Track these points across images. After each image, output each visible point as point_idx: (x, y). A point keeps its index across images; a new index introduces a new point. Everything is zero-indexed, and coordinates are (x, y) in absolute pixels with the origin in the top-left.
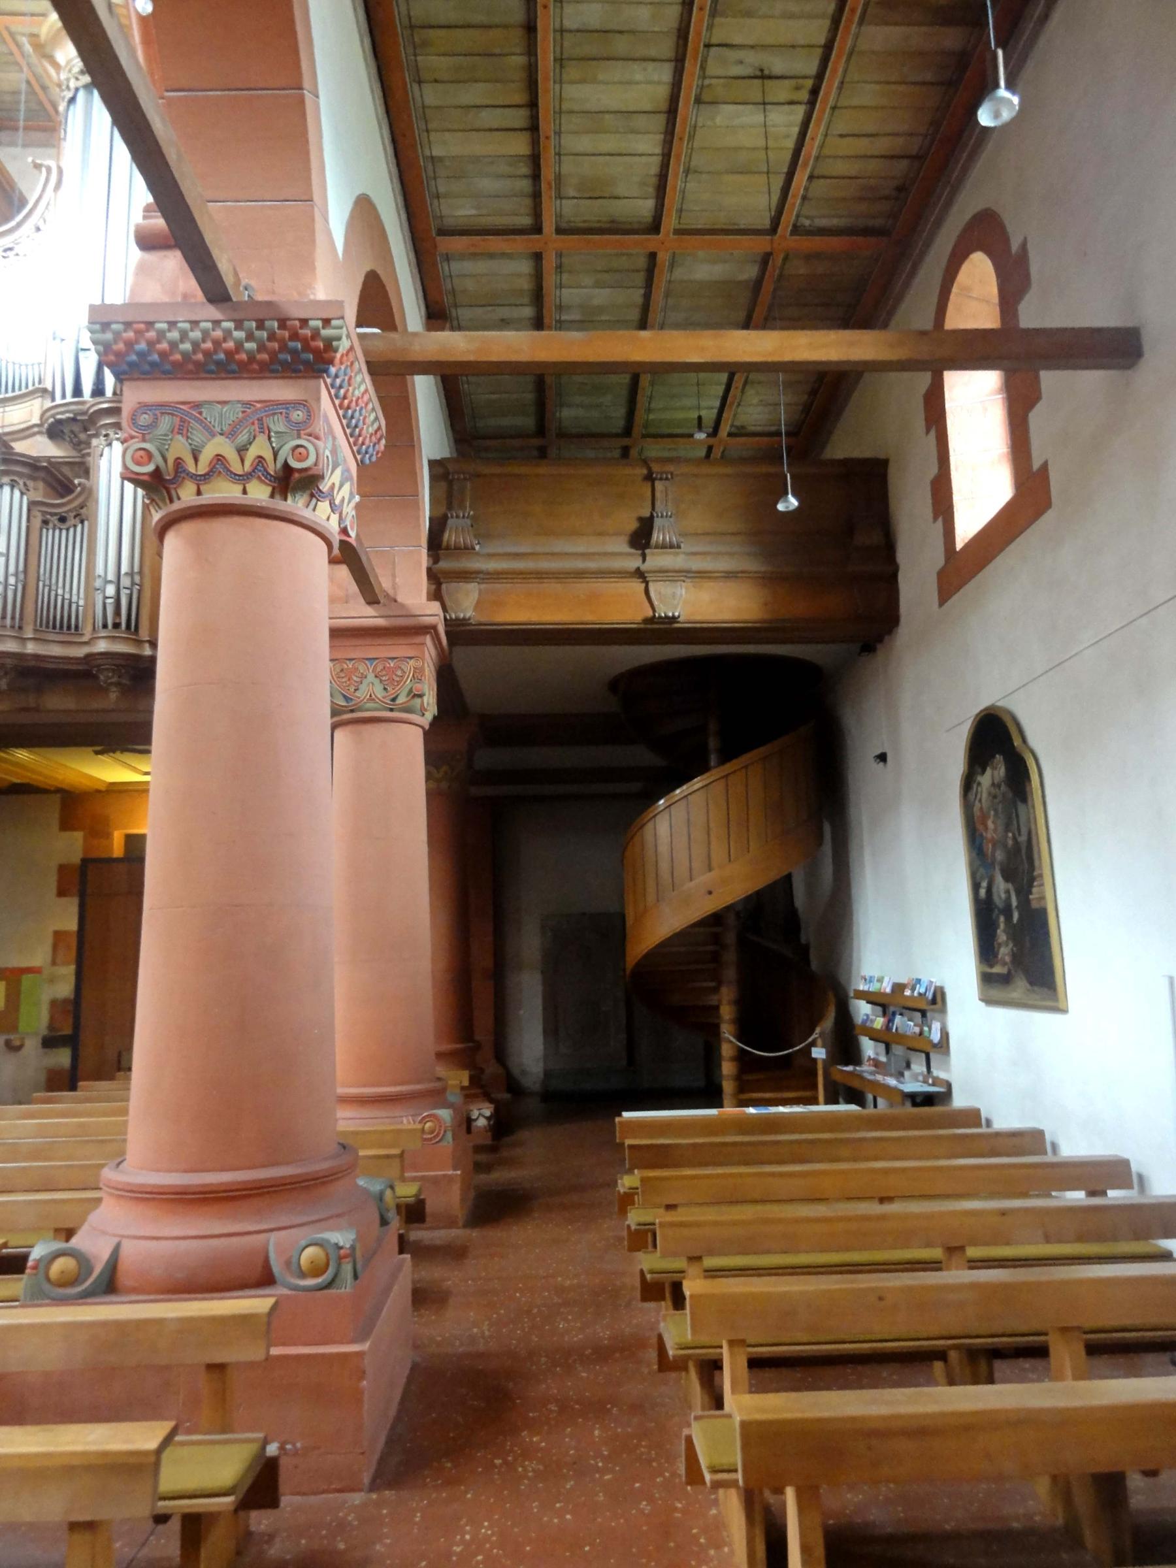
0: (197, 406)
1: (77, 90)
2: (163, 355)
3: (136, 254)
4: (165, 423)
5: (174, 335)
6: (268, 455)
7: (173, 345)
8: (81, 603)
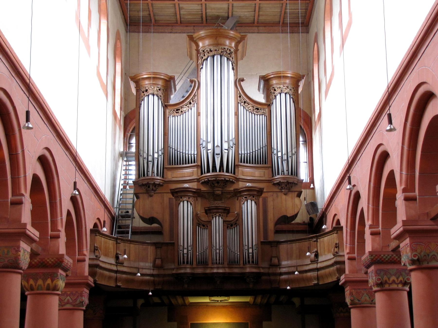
0: (388, 269)
1: (208, 57)
2: (383, 261)
3: (370, 236)
4: (382, 273)
5: (385, 257)
6: (402, 280)
7: (385, 259)
8: (238, 253)
